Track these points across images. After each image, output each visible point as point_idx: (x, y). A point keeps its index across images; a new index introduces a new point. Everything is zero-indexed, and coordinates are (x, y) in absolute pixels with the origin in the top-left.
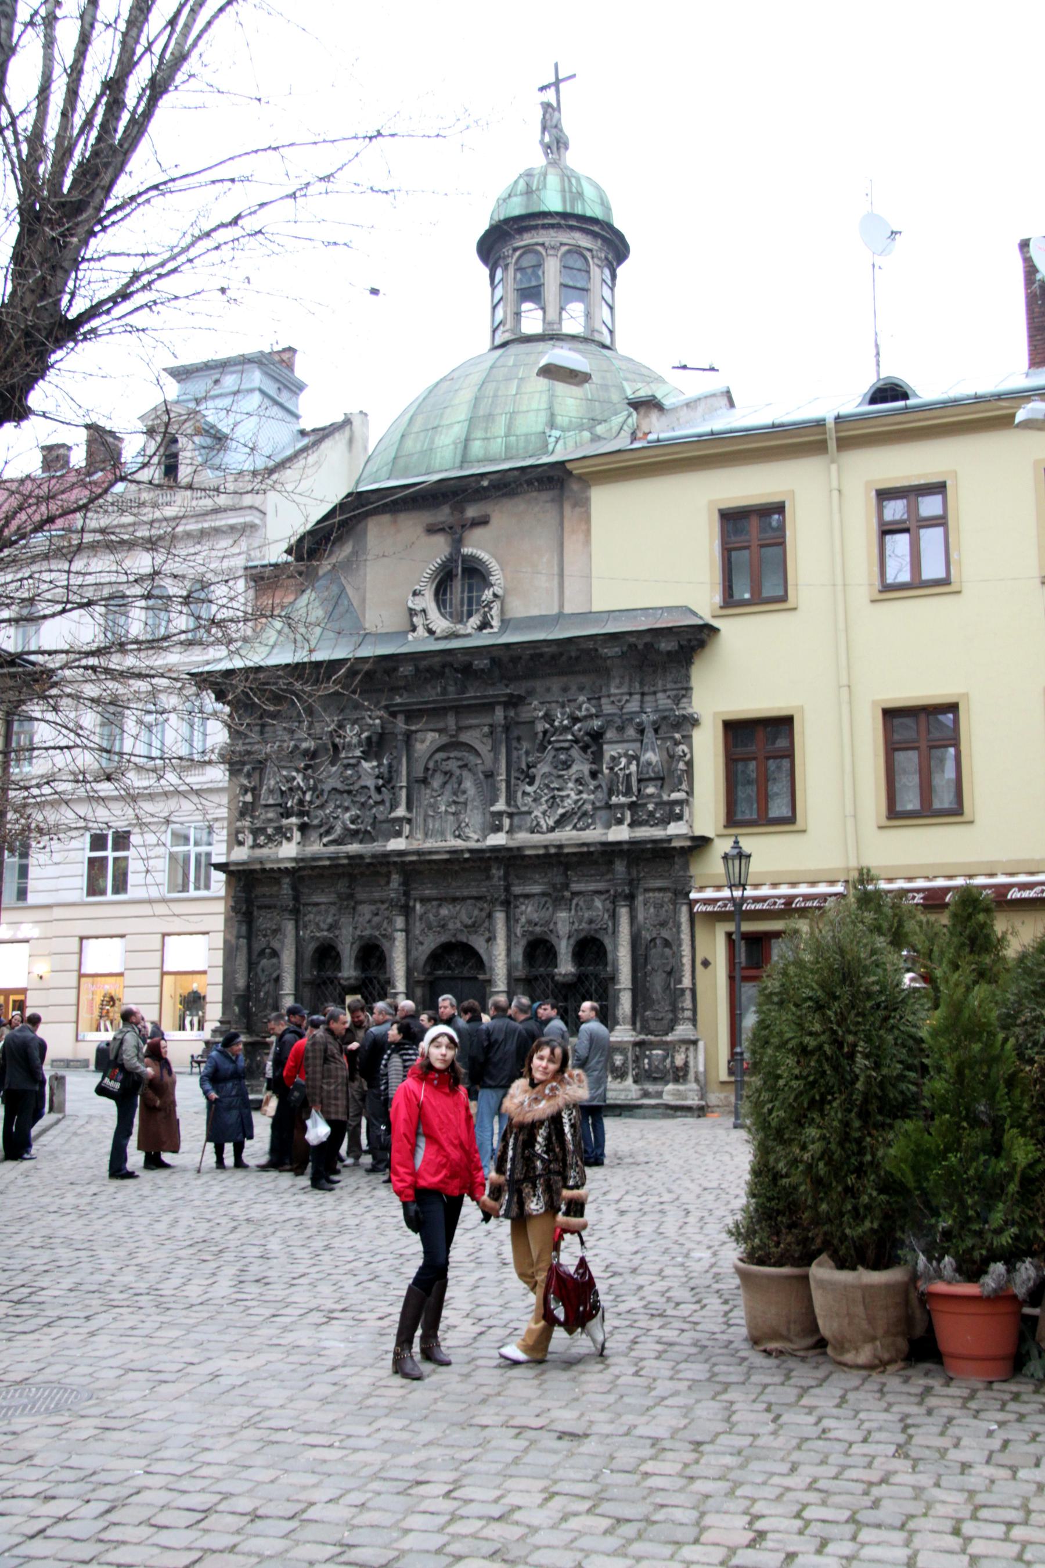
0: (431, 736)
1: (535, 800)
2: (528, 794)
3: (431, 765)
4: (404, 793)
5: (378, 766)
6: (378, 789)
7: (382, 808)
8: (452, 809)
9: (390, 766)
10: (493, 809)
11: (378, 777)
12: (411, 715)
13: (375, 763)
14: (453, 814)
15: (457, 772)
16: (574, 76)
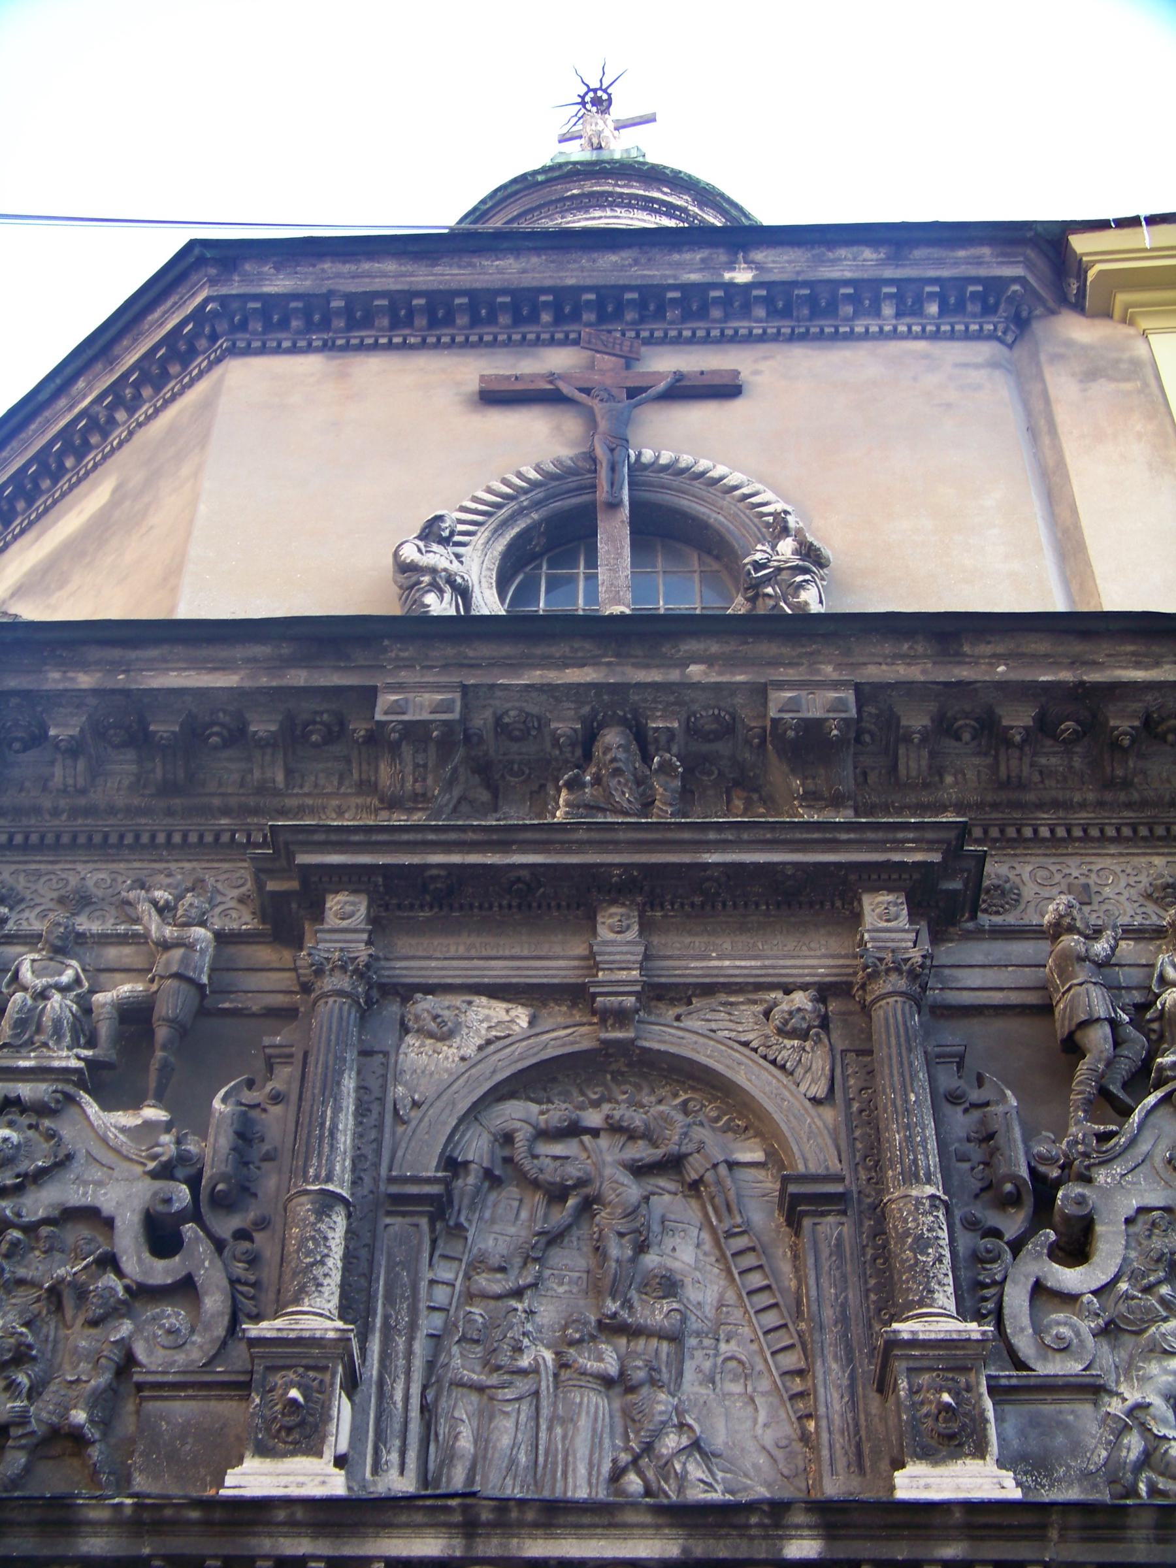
0: (487, 1015)
1: (1109, 1331)
2: (1069, 1299)
3: (477, 1148)
4: (337, 1228)
5: (168, 1127)
6: (162, 1235)
7: (174, 1315)
8: (607, 1358)
9: (246, 1134)
10: (905, 1329)
11: (165, 1172)
12: (409, 898)
13: (153, 1113)
14: (607, 1382)
15: (633, 1191)
16: (650, 119)
